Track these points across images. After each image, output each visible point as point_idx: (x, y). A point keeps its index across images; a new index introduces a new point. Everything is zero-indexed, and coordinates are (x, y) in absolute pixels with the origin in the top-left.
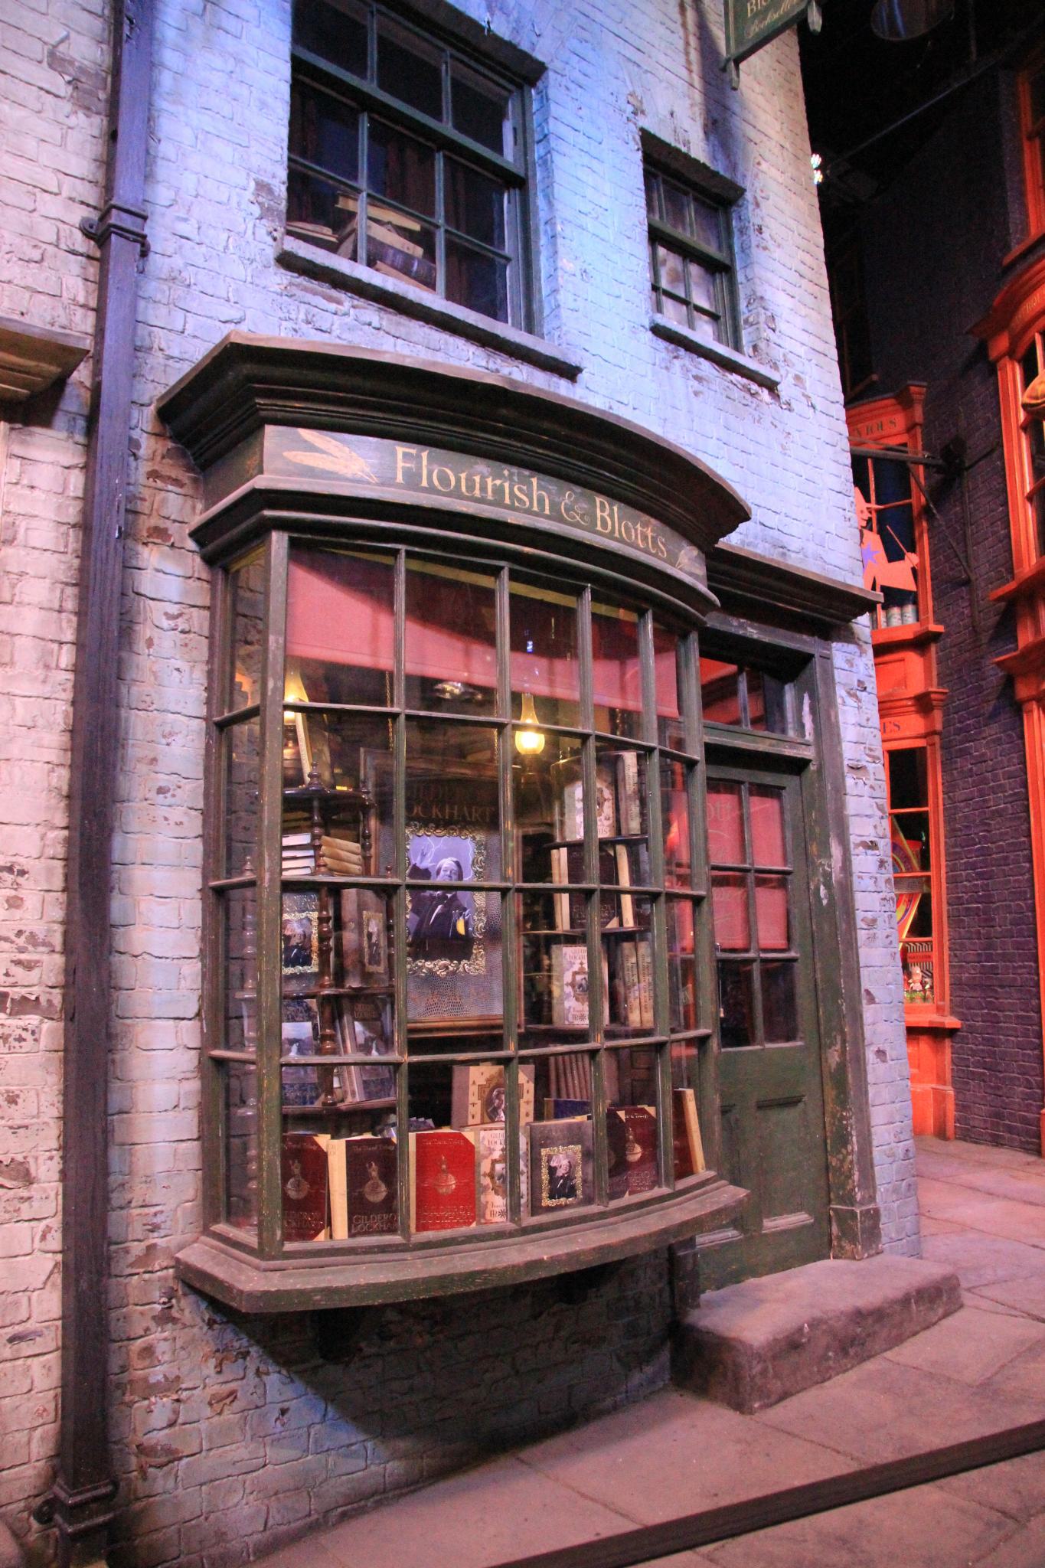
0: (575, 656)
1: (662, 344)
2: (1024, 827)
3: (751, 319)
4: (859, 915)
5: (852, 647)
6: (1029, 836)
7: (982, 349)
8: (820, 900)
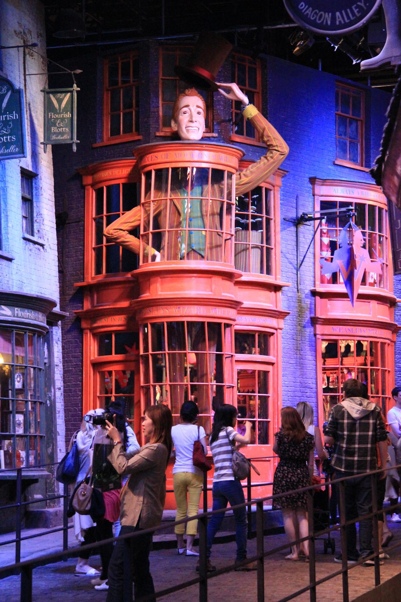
0: (24, 346)
1: (24, 241)
2: (80, 378)
3: (38, 221)
4: (57, 409)
5: (57, 327)
6: (82, 382)
7: (78, 177)
8: (47, 405)
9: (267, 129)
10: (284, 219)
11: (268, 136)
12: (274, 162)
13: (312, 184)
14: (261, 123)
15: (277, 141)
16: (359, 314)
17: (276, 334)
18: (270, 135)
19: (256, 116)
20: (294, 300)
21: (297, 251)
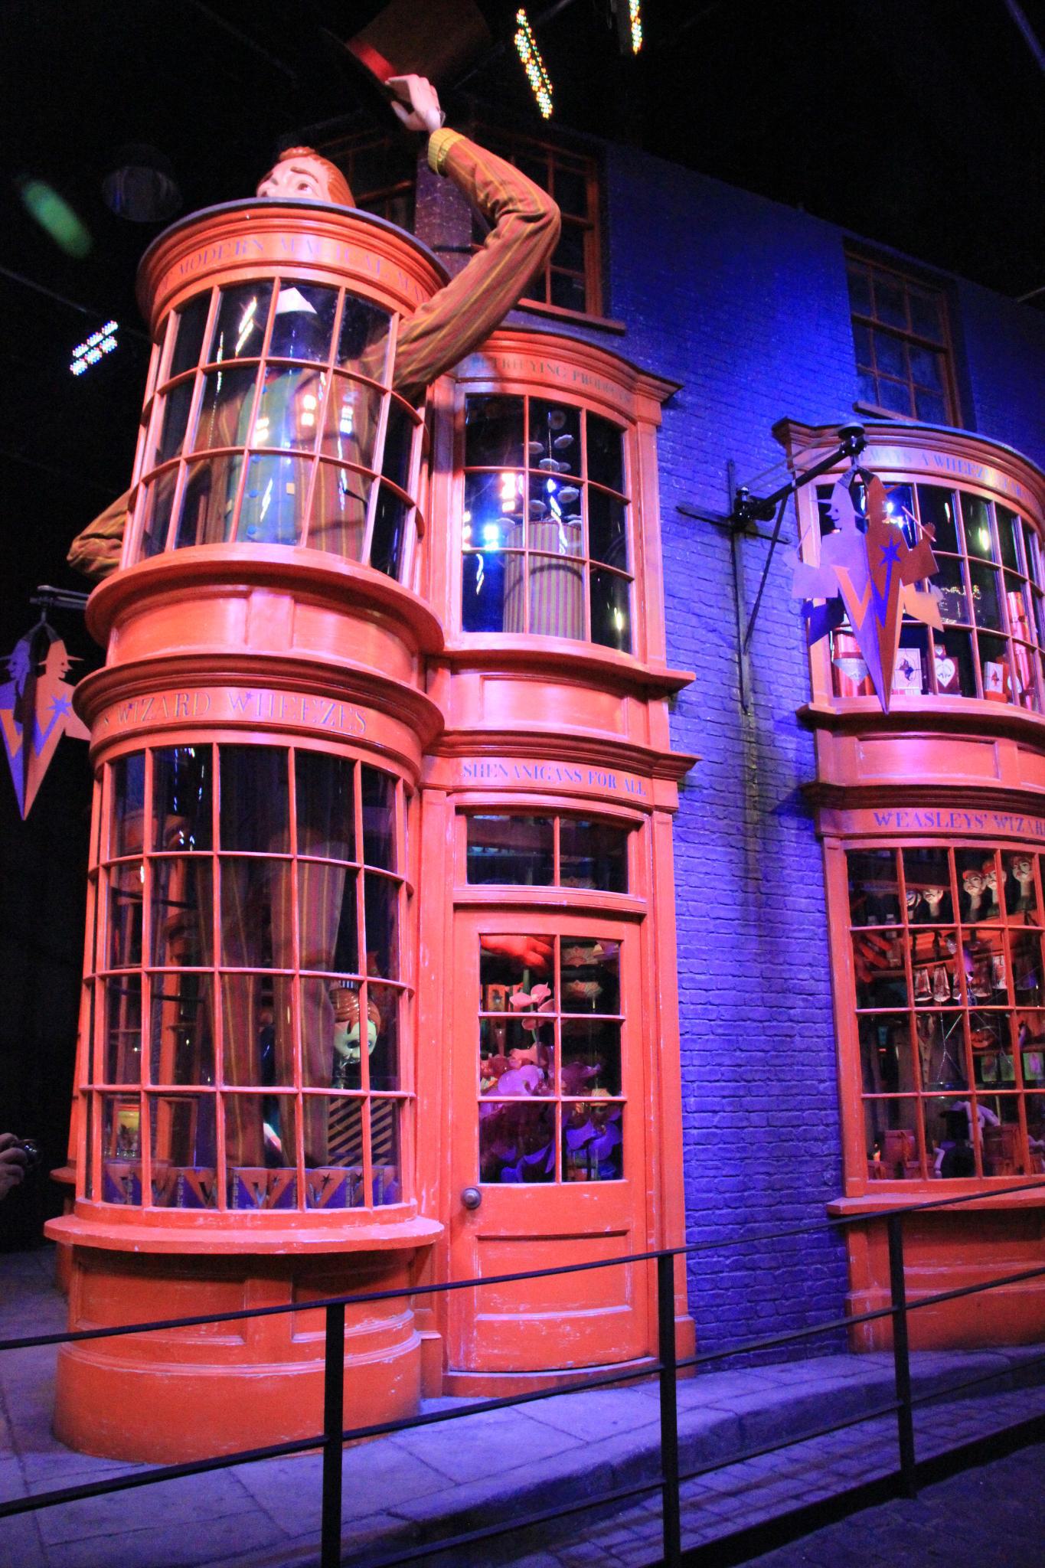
9: (481, 166)
10: (679, 510)
11: (487, 184)
12: (505, 247)
13: (783, 444)
14: (467, 156)
15: (510, 187)
16: (960, 776)
17: (646, 827)
18: (490, 177)
19: (454, 147)
20: (729, 734)
21: (736, 600)
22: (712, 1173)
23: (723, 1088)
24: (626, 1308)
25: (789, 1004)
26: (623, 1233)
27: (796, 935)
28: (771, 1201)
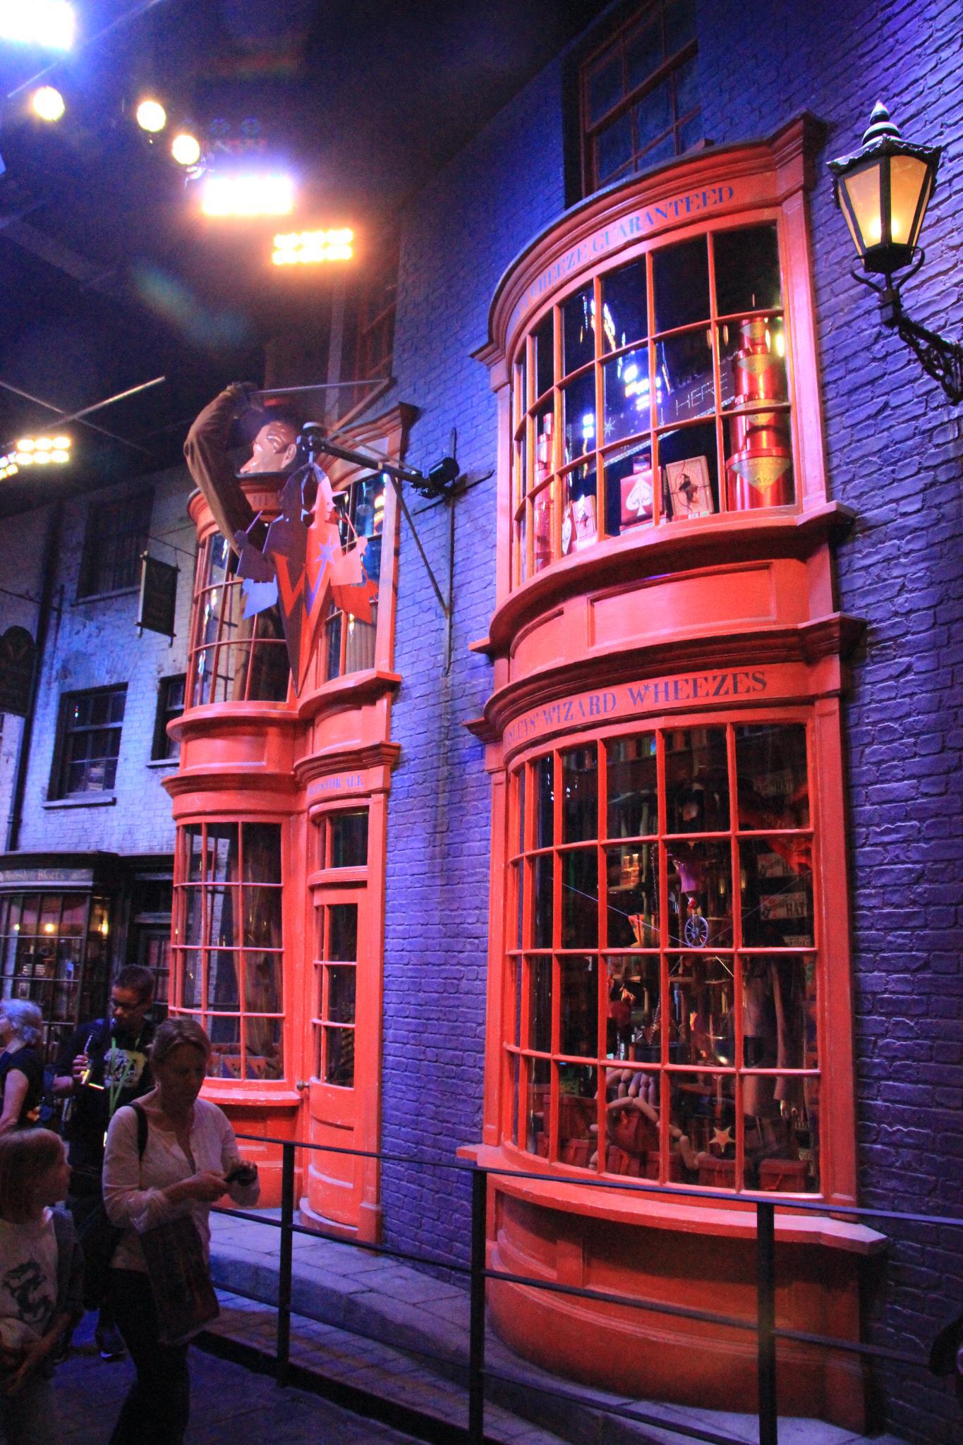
22: (399, 1095)
23: (409, 1024)
24: (351, 1186)
25: (459, 948)
26: (351, 1129)
27: (470, 879)
28: (436, 1131)
